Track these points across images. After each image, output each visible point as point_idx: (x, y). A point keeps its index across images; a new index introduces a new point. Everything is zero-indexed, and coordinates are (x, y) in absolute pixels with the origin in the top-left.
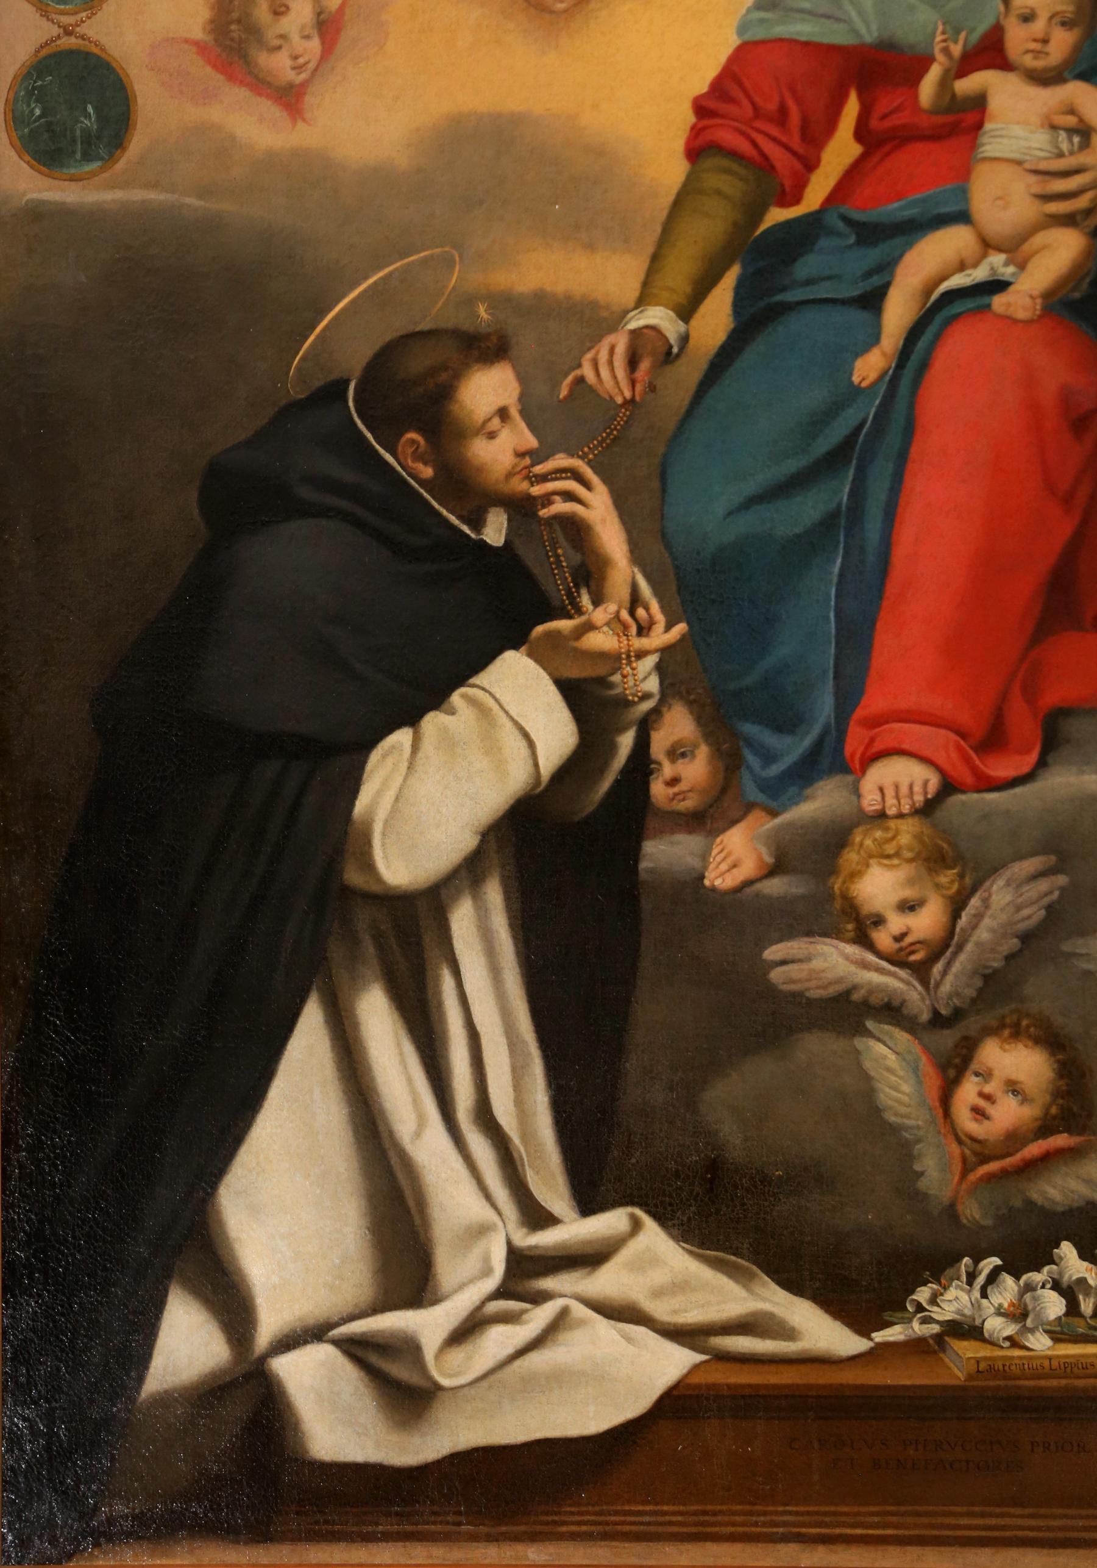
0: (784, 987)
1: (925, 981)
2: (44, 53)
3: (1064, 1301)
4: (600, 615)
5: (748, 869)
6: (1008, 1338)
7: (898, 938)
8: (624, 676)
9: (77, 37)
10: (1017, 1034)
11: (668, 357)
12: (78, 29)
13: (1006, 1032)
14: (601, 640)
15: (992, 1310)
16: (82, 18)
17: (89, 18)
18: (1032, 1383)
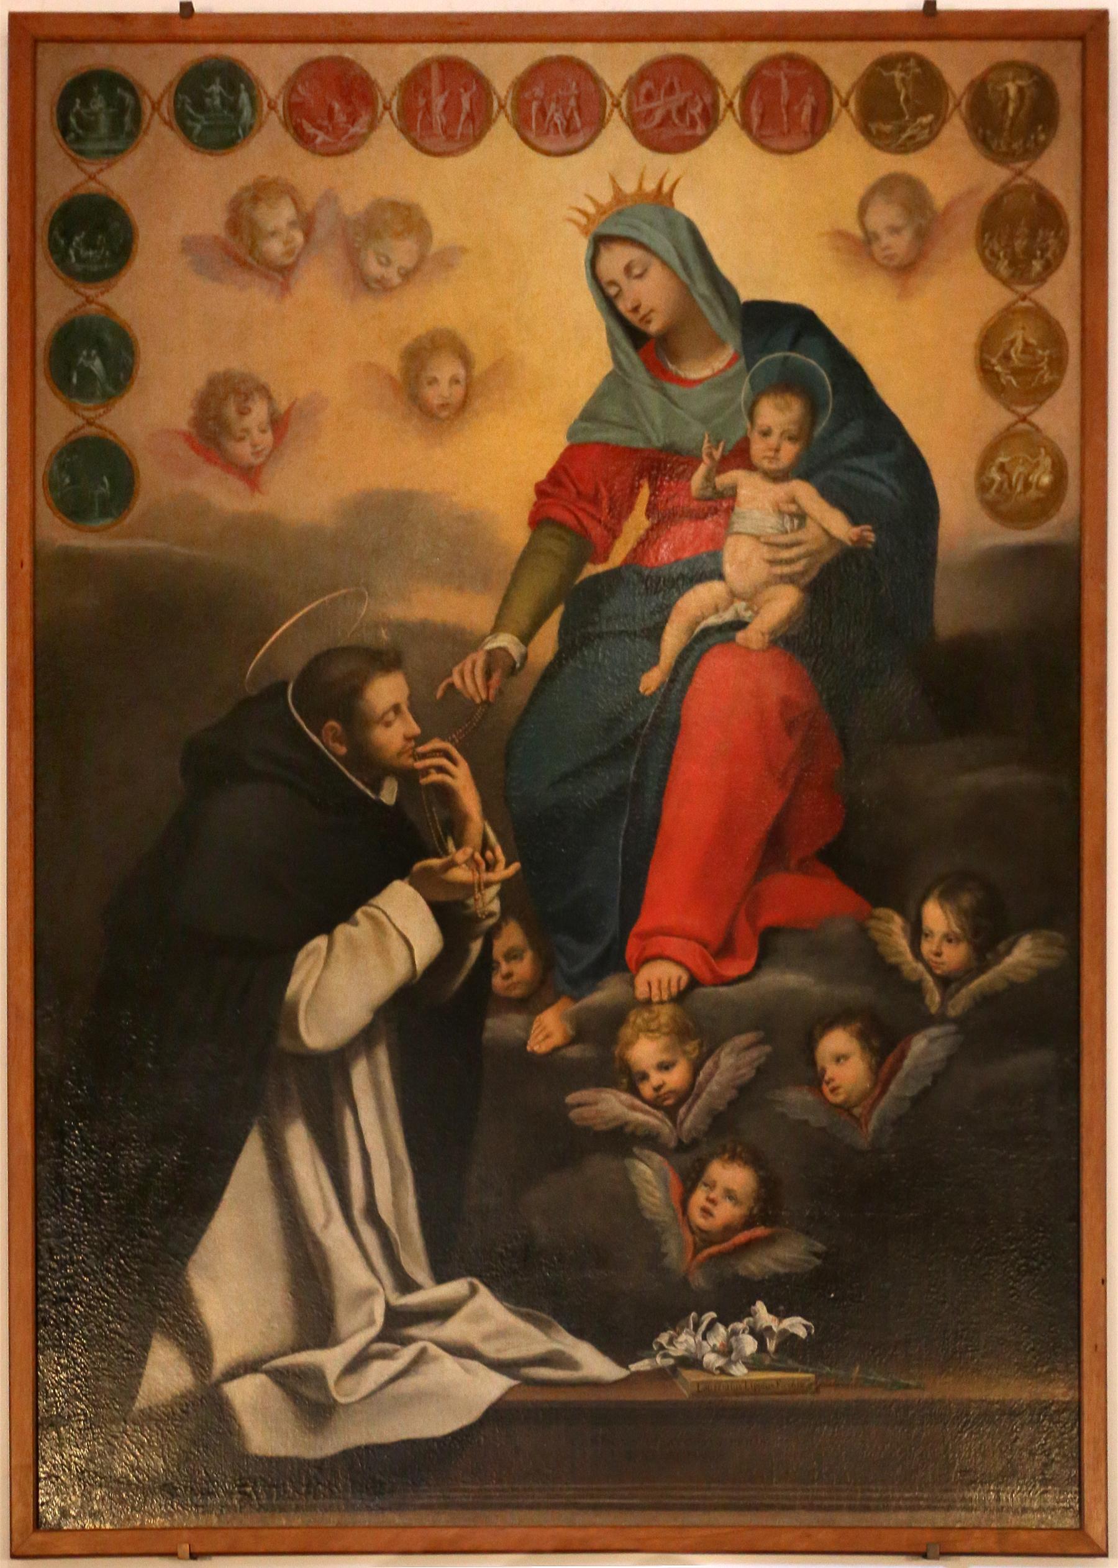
0: (577, 1123)
1: (673, 1119)
2: (73, 437)
3: (756, 1343)
4: (460, 856)
5: (557, 1039)
6: (719, 1368)
7: (657, 1089)
8: (476, 900)
10: (734, 1157)
11: (512, 671)
13: (727, 1156)
14: (461, 874)
15: (709, 1349)
18: (734, 1398)
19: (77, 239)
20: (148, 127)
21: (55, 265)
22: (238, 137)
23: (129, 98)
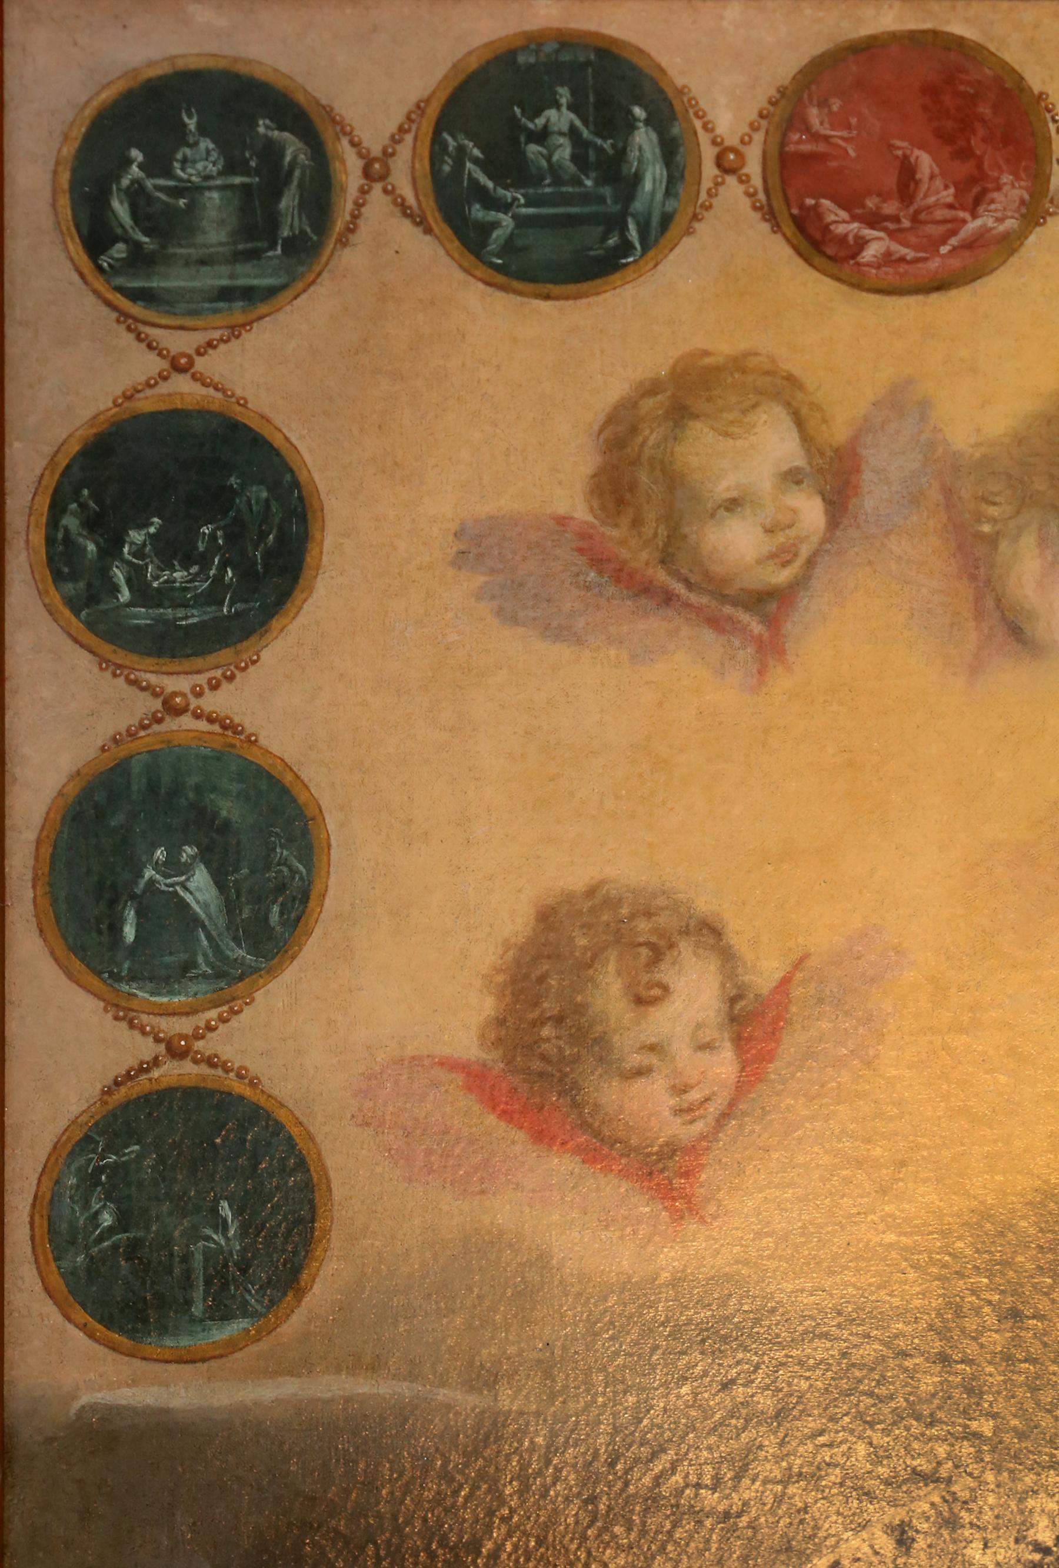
9: (196, 1062)
12: (199, 1045)
16: (208, 1022)
17: (225, 1021)
19: (136, 536)
20: (351, 228)
21: (67, 613)
22: (626, 247)
23: (293, 147)
